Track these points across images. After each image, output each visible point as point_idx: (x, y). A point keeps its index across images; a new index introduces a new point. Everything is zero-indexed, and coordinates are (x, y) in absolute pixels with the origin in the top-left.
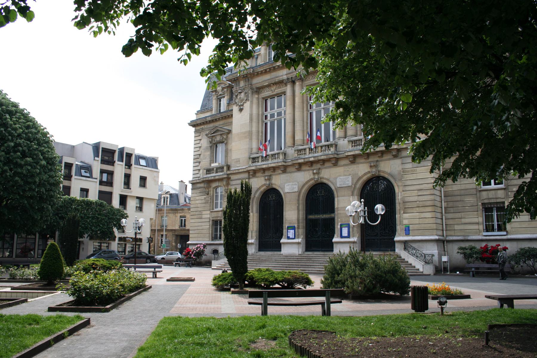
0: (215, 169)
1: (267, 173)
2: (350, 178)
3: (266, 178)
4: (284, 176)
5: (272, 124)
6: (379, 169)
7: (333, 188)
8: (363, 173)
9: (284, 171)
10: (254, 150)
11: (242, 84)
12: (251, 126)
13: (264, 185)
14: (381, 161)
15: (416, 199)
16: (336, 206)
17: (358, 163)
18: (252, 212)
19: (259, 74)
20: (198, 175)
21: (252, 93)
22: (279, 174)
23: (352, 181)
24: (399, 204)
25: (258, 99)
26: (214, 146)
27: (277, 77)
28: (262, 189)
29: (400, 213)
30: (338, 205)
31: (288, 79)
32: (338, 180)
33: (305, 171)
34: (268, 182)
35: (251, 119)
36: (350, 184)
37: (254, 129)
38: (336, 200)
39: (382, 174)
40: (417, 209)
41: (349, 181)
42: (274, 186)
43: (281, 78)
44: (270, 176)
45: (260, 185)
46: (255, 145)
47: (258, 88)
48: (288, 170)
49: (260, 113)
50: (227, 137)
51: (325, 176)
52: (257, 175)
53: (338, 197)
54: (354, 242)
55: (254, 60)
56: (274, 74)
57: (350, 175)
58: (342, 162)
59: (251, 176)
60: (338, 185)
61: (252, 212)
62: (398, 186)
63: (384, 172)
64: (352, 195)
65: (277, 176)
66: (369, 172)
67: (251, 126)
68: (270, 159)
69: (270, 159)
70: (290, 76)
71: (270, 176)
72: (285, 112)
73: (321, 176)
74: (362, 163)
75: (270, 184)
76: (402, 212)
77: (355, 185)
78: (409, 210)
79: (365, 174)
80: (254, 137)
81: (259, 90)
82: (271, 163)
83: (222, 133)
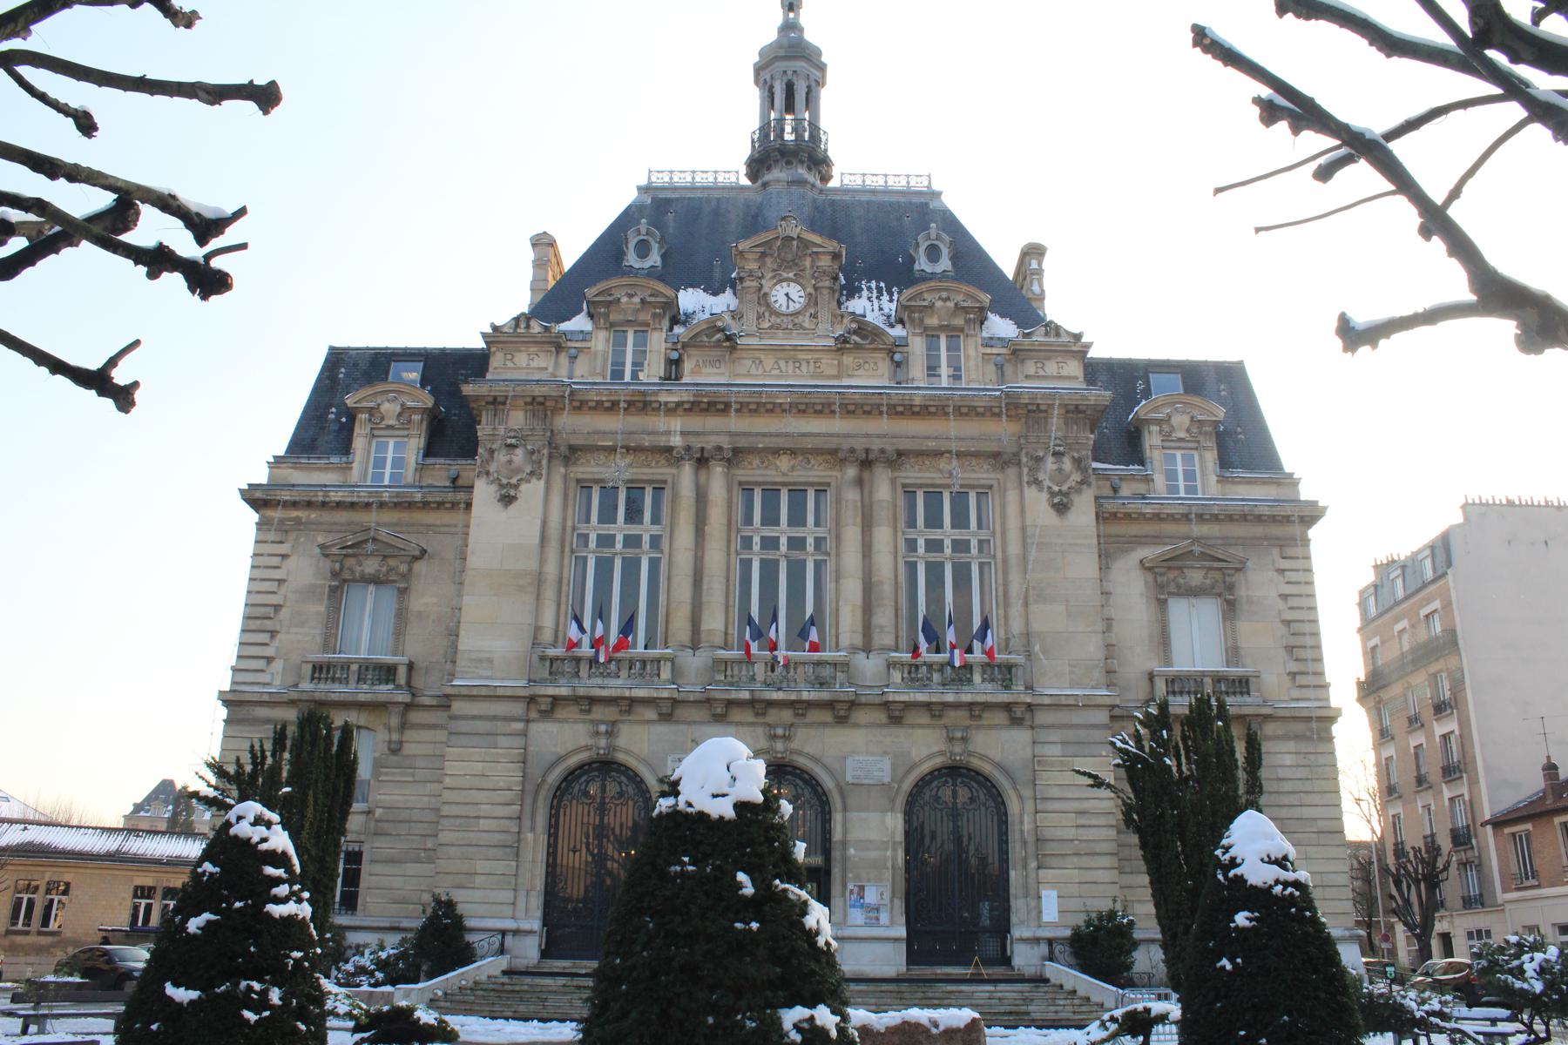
0: (355, 667)
1: (598, 713)
2: (886, 764)
3: (603, 728)
4: (662, 730)
5: (631, 567)
6: (971, 748)
7: (828, 783)
8: (925, 752)
9: (666, 718)
10: (547, 636)
11: (517, 418)
12: (542, 561)
13: (587, 748)
14: (978, 727)
15: (1071, 833)
16: (837, 836)
17: (912, 726)
18: (533, 829)
19: (581, 406)
20: (265, 678)
21: (550, 457)
22: (648, 722)
23: (894, 767)
24: (1024, 843)
25: (565, 477)
26: (339, 585)
27: (649, 433)
28: (573, 761)
29: (1025, 867)
30: (845, 833)
31: (688, 448)
32: (849, 762)
33: (738, 724)
34: (603, 742)
35: (544, 539)
36: (887, 780)
37: (551, 569)
38: (837, 818)
39: (976, 763)
40: (1075, 859)
41: (882, 770)
42: (621, 757)
43: (662, 441)
44: (614, 723)
45: (570, 746)
46: (548, 621)
47: (573, 449)
48: (681, 712)
49: (569, 524)
50: (410, 570)
51: (808, 749)
52: (559, 713)
53: (845, 809)
54: (896, 940)
55: (564, 359)
56: (636, 421)
57: (885, 753)
58: (861, 716)
59: (534, 715)
60: (849, 779)
61: (533, 829)
62: (1021, 798)
63: (983, 757)
64: (892, 810)
65: (638, 729)
66: (942, 753)
67: (542, 561)
68: (624, 673)
69: (624, 673)
70: (697, 443)
71: (614, 723)
72: (655, 542)
73: (794, 745)
74: (921, 726)
75: (612, 748)
76: (1033, 864)
77: (901, 781)
78: (1054, 862)
79: (930, 757)
80: (549, 593)
81: (572, 453)
82: (617, 686)
83: (390, 551)
